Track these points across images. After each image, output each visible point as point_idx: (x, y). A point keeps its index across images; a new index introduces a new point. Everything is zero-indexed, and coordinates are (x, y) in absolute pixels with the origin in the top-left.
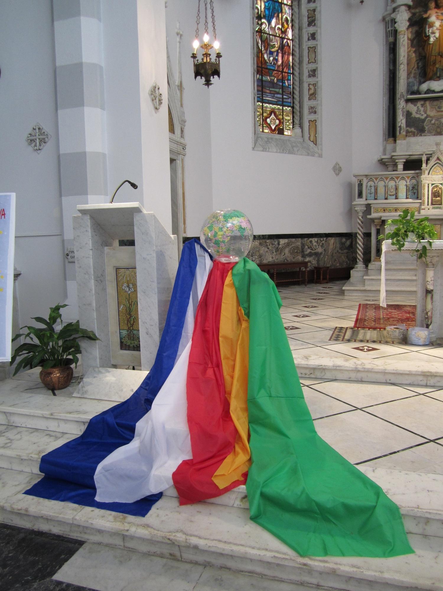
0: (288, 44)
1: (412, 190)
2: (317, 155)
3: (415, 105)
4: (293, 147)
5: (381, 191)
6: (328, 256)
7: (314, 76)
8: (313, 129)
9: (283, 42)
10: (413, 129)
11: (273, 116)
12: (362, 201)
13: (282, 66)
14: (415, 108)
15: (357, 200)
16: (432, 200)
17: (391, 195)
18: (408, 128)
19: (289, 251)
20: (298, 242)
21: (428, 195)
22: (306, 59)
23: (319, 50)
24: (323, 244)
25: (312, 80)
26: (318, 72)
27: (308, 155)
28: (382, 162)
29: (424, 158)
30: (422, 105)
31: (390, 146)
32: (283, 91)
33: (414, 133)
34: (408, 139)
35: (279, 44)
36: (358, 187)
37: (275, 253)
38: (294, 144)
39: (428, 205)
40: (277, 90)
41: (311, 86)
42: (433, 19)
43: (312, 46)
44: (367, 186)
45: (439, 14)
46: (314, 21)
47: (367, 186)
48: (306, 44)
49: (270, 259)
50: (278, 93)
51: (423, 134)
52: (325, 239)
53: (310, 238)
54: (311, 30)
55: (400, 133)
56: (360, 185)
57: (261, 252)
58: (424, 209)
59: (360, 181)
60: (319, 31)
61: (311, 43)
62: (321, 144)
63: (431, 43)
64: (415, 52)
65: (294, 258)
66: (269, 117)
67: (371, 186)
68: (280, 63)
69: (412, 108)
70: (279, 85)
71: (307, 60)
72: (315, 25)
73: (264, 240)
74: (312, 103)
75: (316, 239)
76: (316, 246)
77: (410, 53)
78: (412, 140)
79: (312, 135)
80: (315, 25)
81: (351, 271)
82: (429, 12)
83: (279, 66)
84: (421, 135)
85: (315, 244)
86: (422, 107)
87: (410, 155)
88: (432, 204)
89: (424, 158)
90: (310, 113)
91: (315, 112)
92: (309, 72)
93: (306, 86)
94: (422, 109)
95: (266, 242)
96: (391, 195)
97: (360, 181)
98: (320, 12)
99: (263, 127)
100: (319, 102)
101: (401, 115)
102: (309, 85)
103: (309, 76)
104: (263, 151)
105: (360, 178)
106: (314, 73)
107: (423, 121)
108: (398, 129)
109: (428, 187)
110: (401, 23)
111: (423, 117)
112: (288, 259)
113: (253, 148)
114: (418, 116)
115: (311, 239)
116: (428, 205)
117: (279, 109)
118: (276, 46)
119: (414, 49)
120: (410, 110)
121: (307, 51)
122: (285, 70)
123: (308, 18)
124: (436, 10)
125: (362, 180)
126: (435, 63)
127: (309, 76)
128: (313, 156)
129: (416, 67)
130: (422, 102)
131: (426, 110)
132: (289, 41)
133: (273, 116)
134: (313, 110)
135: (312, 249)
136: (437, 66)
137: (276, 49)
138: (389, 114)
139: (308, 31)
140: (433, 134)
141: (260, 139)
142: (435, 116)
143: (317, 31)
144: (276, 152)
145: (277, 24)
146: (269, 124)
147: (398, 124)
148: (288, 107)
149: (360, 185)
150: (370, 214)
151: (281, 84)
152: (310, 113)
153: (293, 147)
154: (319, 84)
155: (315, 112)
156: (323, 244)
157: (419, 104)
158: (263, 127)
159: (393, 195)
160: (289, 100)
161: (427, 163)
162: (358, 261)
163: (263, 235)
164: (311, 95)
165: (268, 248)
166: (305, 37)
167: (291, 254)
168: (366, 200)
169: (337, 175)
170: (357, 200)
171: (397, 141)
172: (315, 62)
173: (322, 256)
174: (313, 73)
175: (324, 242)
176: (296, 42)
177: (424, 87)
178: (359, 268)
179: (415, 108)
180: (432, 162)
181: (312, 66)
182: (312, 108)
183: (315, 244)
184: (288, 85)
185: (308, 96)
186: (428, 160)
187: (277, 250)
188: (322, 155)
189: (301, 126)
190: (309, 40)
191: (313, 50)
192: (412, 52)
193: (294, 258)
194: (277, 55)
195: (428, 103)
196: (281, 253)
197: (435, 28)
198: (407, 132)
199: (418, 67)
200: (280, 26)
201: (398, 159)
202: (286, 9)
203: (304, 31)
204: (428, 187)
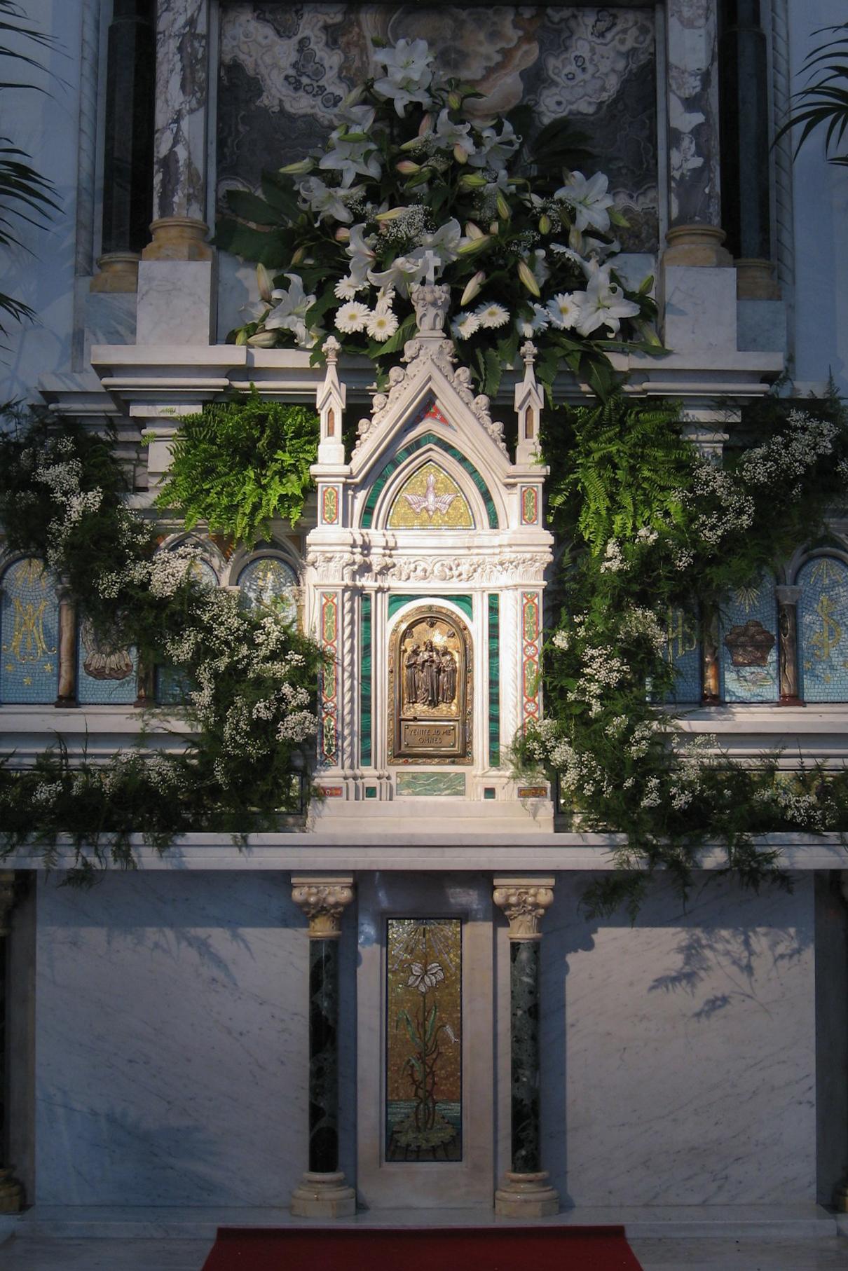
3: (283, 32)
14: (284, 53)
16: (398, 722)
30: (333, 35)
55: (166, 209)
86: (332, 43)
87: (233, 372)
88: (400, 754)
94: (332, 60)
96: (99, 674)
101: (176, 81)
108: (158, 179)
114: (302, 104)
116: (366, 756)
120: (248, 63)
138: (111, 84)
147: (162, 147)
161: (350, 440)
171: (143, 265)
179: (284, 53)
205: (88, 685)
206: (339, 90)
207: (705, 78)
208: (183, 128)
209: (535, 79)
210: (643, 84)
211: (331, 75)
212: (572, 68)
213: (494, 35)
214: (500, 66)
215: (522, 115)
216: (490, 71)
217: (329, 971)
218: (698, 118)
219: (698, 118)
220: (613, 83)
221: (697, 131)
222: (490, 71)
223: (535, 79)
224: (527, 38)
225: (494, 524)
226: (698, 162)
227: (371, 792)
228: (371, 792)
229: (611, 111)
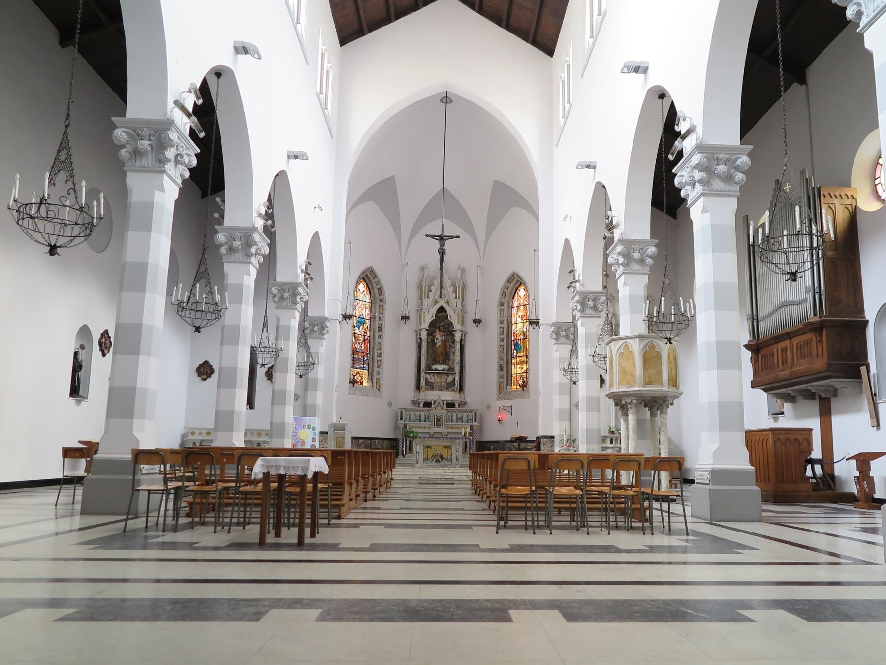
5: (412, 417)
12: (402, 422)
20: (369, 442)
25: (379, 358)
26: (382, 355)
28: (413, 402)
31: (417, 394)
48: (377, 340)
54: (380, 333)
56: (402, 413)
61: (379, 340)
69: (428, 377)
74: (378, 370)
93: (375, 361)
134: (379, 374)
139: (377, 334)
149: (402, 413)
166: (376, 337)
174: (380, 355)
177: (434, 367)
181: (379, 351)
189: (372, 381)
191: (380, 343)
202: (367, 321)
208: (423, 383)
210: (454, 380)
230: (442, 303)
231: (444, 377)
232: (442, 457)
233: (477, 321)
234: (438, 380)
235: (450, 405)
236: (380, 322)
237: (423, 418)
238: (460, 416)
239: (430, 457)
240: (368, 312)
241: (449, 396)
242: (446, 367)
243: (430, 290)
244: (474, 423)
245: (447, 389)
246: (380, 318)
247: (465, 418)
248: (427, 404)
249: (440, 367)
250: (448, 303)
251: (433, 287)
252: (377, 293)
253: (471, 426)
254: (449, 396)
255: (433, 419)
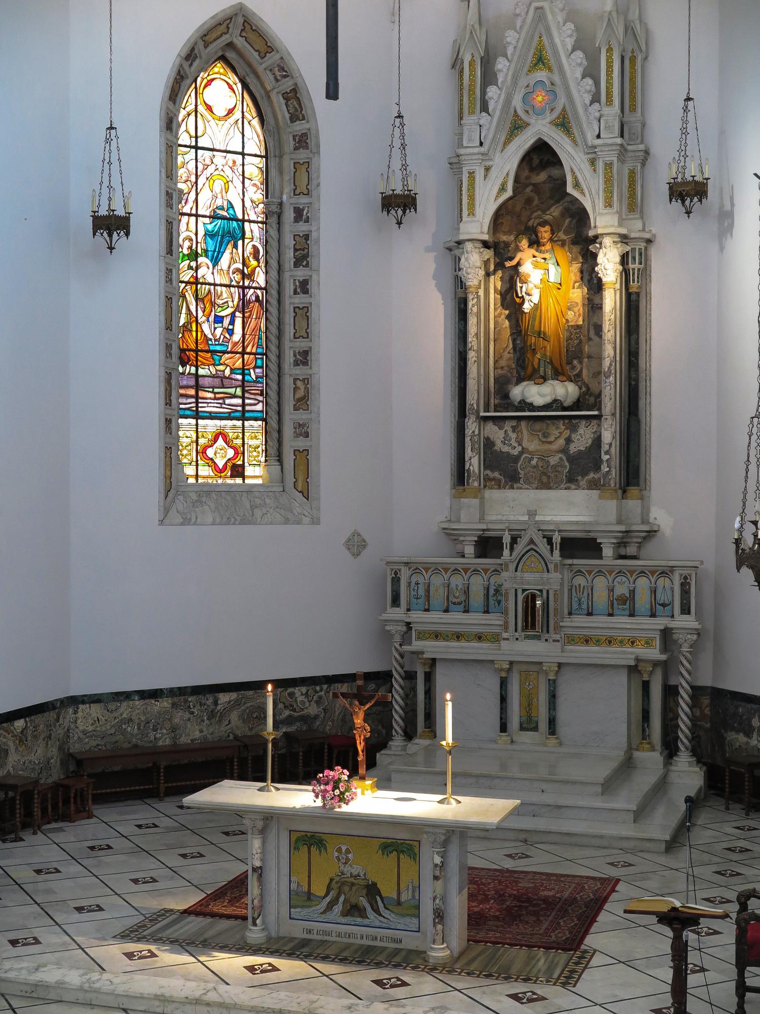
0: (257, 297)
1: (495, 595)
2: (306, 520)
4: (253, 507)
6: (333, 721)
7: (305, 363)
8: (302, 468)
9: (244, 295)
10: (496, 474)
11: (220, 441)
12: (397, 614)
13: (243, 342)
14: (501, 434)
15: (389, 610)
17: (454, 603)
18: (488, 472)
19: (241, 717)
21: (516, 610)
22: (289, 331)
23: (314, 314)
24: (320, 697)
25: (300, 371)
26: (313, 356)
27: (287, 521)
29: (507, 539)
30: (514, 429)
32: (244, 391)
33: (500, 481)
34: (488, 493)
35: (236, 300)
36: (392, 584)
37: (207, 722)
38: (258, 501)
39: (516, 631)
40: (232, 391)
41: (299, 383)
42: (527, 268)
43: (301, 306)
44: (410, 583)
45: (539, 259)
46: (305, 257)
47: (410, 583)
48: (291, 301)
49: (197, 734)
50: (234, 396)
51: (515, 486)
52: (325, 686)
53: (290, 687)
56: (396, 581)
57: (176, 720)
58: (507, 639)
59: (396, 573)
60: (314, 277)
61: (300, 300)
62: (318, 499)
63: (526, 311)
64: (508, 317)
65: (251, 729)
66: (212, 446)
67: (417, 584)
68: (237, 337)
70: (237, 380)
71: (293, 331)
72: (307, 265)
73: (182, 698)
74: (301, 416)
75: (304, 690)
76: (303, 702)
77: (500, 320)
78: (493, 495)
79: (301, 479)
80: (307, 265)
81: (378, 754)
82: (519, 256)
83: (236, 344)
84: (512, 487)
85: (301, 699)
86: (514, 431)
87: (483, 530)
89: (507, 539)
90: (297, 435)
91: (307, 435)
92: (295, 355)
93: (288, 382)
94: (513, 436)
95: (186, 701)
96: (454, 603)
97: (396, 573)
98: (318, 241)
99: (197, 465)
100: (313, 416)
101: (470, 448)
102: (295, 380)
103: (296, 363)
104: (182, 524)
105: (396, 567)
106: (306, 358)
107: (516, 459)
109: (516, 595)
110: (468, 274)
111: (515, 452)
112: (239, 733)
113: (161, 522)
114: (505, 449)
115: (290, 690)
116: (516, 631)
117: (234, 427)
118: (230, 304)
119: (507, 312)
120: (491, 437)
121: (293, 314)
122: (248, 350)
123: (296, 250)
124: (533, 251)
125: (400, 570)
126: (534, 351)
127: (296, 363)
128: (299, 523)
129: (511, 346)
130: (514, 423)
131: (522, 439)
132: (259, 292)
133: (220, 441)
134: (303, 431)
135: (294, 710)
136: (538, 356)
137: (230, 311)
140: (534, 486)
141: (181, 498)
142: (537, 451)
143: (311, 276)
144: (213, 524)
145: (233, 260)
146: (212, 459)
148: (256, 419)
149: (396, 581)
150: (410, 644)
151: (240, 377)
152: (297, 435)
153: (253, 507)
154: (314, 381)
155: (307, 435)
156: (320, 697)
157: (508, 426)
158: (197, 465)
159: (460, 604)
160: (259, 407)
161: (512, 549)
162: (394, 733)
163: (180, 688)
164: (299, 400)
165: (192, 713)
166: (289, 287)
167: (244, 721)
168: (408, 610)
169: (356, 555)
170: (389, 610)
172: (307, 336)
173: (318, 723)
174: (304, 358)
175: (323, 693)
176: (271, 295)
177: (517, 392)
178: (393, 748)
179: (501, 434)
180: (520, 548)
181: (302, 344)
182: (300, 425)
183: (301, 699)
184: (257, 377)
185: (292, 403)
186: (514, 540)
187: (212, 715)
188: (319, 519)
189: (280, 460)
190: (295, 292)
191: (304, 313)
192: (503, 316)
193: (251, 729)
194: (232, 322)
195: (523, 424)
196: (220, 721)
197: (531, 285)
198: (487, 479)
199: (514, 348)
200: (240, 266)
201: (464, 535)
202: (254, 231)
203: (287, 275)
204: (516, 595)
205: (452, 606)
206: (516, 445)
207: (610, 445)
209: (569, 440)
211: (513, 440)
212: (579, 437)
213: (557, 428)
214: (559, 437)
215: (564, 451)
216: (556, 438)
217: (504, 683)
218: (608, 457)
219: (608, 457)
220: (590, 441)
221: (607, 461)
222: (556, 438)
223: (569, 440)
224: (566, 429)
225: (548, 571)
226: (607, 469)
227: (517, 639)
228: (517, 639)
229: (589, 449)
230: (543, 128)
231: (558, 434)
232: (372, 890)
233: (688, 192)
234: (533, 445)
235: (579, 546)
236: (302, 227)
237: (477, 597)
238: (621, 590)
239: (319, 889)
240: (255, 194)
241: (571, 509)
242: (566, 391)
243: (489, 77)
244: (683, 623)
245: (572, 480)
246: (299, 214)
247: (643, 601)
248: (488, 545)
249: (537, 393)
250: (563, 124)
251: (501, 64)
252: (283, 114)
253: (666, 633)
254: (571, 509)
255: (514, 606)
